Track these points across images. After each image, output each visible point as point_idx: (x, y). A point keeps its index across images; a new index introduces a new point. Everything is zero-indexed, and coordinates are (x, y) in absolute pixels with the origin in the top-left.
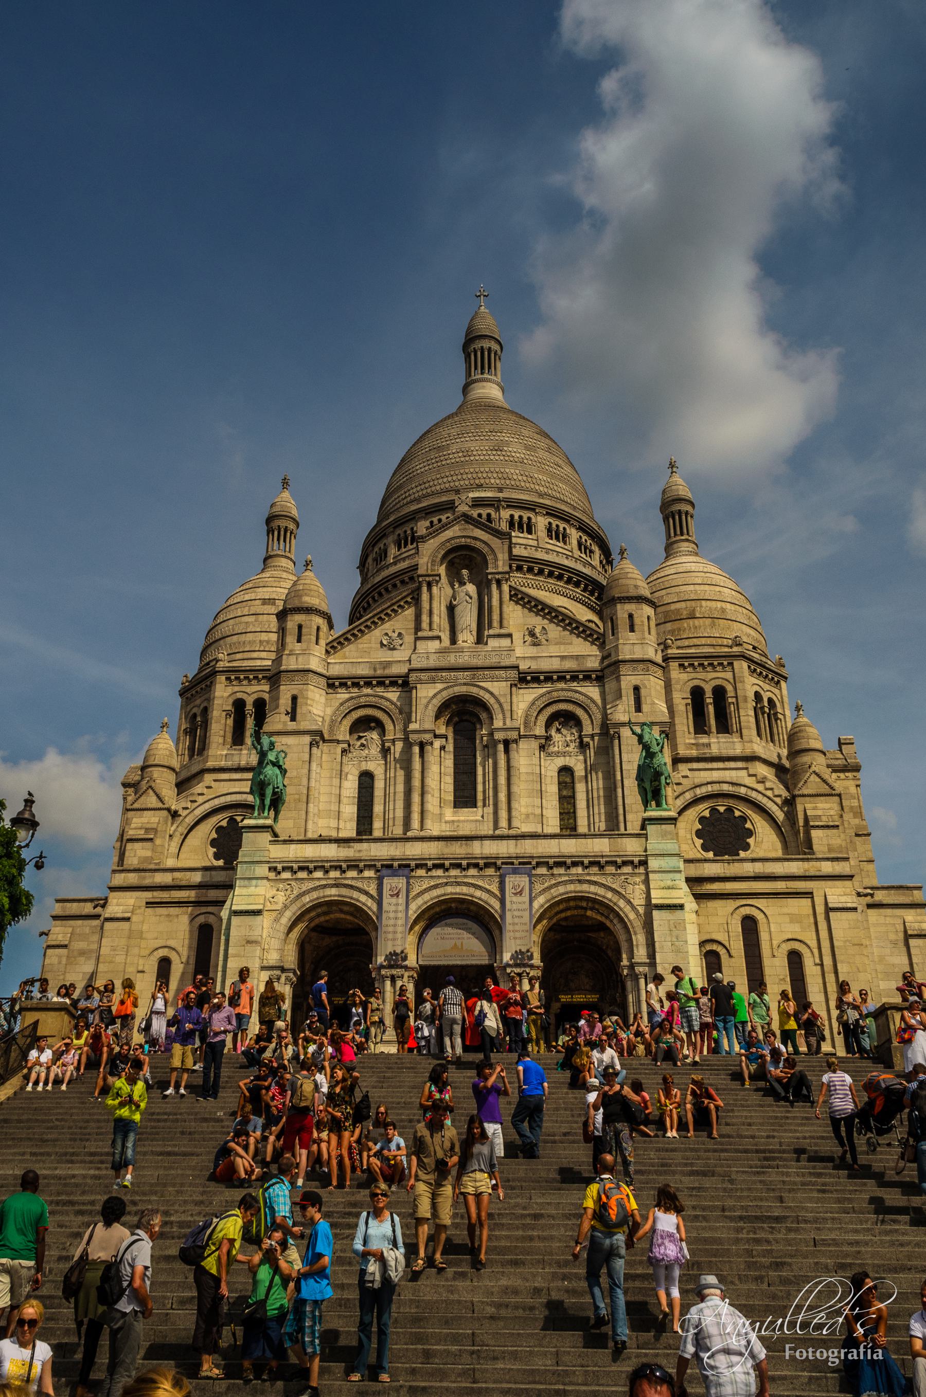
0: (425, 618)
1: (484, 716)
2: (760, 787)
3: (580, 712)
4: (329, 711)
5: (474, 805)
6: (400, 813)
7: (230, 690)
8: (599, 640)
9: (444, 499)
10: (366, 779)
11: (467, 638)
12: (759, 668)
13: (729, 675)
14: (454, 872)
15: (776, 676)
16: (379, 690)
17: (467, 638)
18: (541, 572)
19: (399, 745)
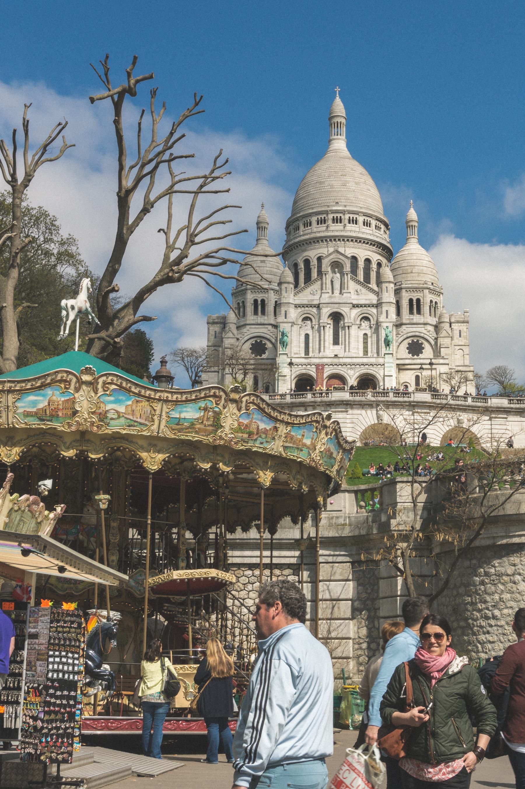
0: (324, 286)
1: (342, 318)
2: (428, 333)
3: (370, 317)
4: (296, 315)
5: (338, 344)
6: (317, 346)
7: (252, 296)
8: (377, 294)
9: (323, 209)
10: (307, 336)
11: (337, 292)
12: (433, 291)
13: (422, 295)
14: (335, 366)
15: (439, 294)
16: (311, 308)
17: (337, 292)
18: (360, 242)
19: (317, 326)
